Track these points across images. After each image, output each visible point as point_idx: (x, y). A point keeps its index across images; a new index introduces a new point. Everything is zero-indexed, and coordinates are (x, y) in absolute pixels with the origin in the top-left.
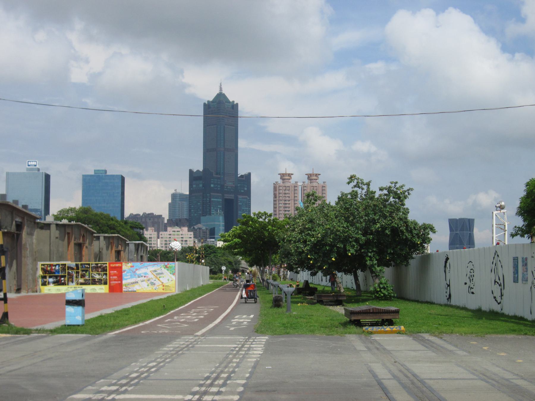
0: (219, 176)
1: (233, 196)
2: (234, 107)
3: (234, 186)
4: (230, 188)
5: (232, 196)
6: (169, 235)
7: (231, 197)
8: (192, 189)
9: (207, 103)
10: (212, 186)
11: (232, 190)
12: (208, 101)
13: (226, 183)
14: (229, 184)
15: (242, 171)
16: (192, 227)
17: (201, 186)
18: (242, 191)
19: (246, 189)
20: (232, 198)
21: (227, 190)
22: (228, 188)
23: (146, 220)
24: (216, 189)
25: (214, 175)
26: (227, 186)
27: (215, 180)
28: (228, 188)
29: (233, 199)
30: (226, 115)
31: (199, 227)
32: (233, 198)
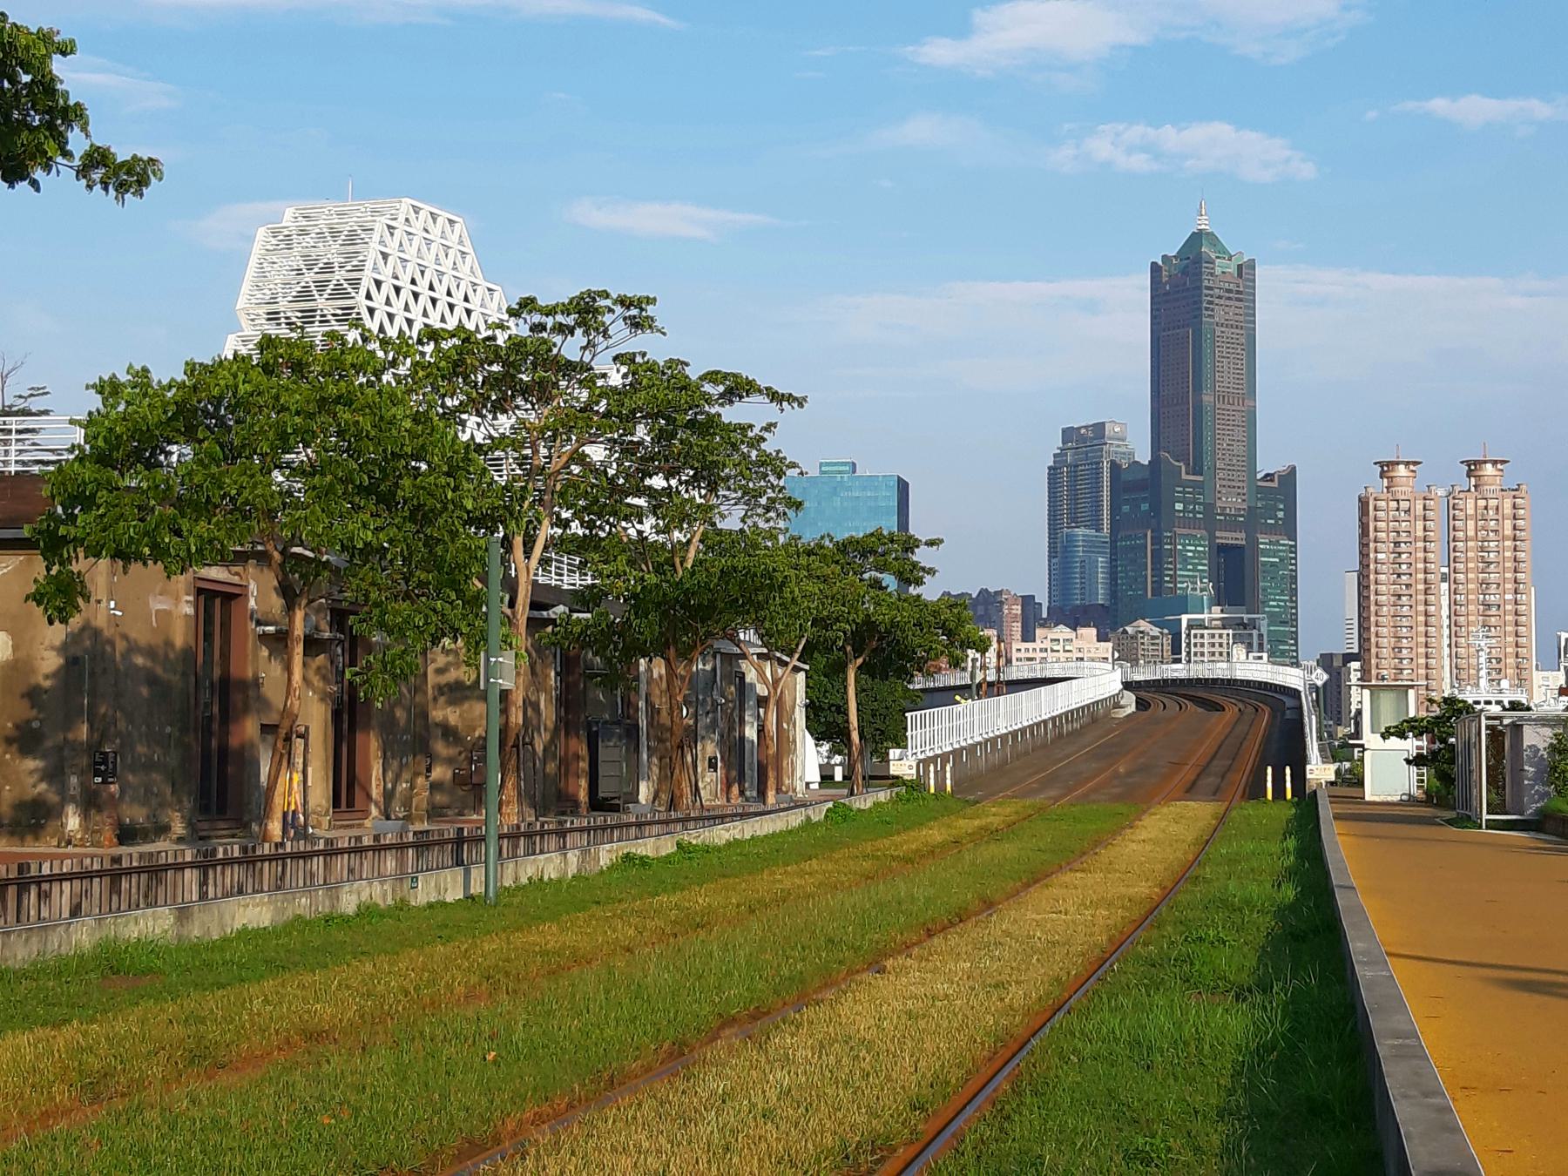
0: (1200, 478)
2: (1246, 271)
4: (1233, 512)
5: (1238, 535)
6: (1041, 650)
7: (1236, 539)
8: (1118, 518)
9: (1160, 263)
10: (1179, 506)
11: (1242, 519)
12: (1164, 257)
13: (1219, 498)
14: (1231, 502)
15: (1267, 463)
16: (1121, 629)
17: (1145, 507)
18: (1269, 521)
19: (1281, 514)
21: (1222, 518)
22: (1228, 511)
23: (986, 610)
24: (1191, 515)
25: (1184, 476)
26: (1225, 508)
27: (1187, 490)
28: (1228, 511)
29: (1241, 548)
30: (1220, 297)
31: (1141, 629)
32: (1244, 543)
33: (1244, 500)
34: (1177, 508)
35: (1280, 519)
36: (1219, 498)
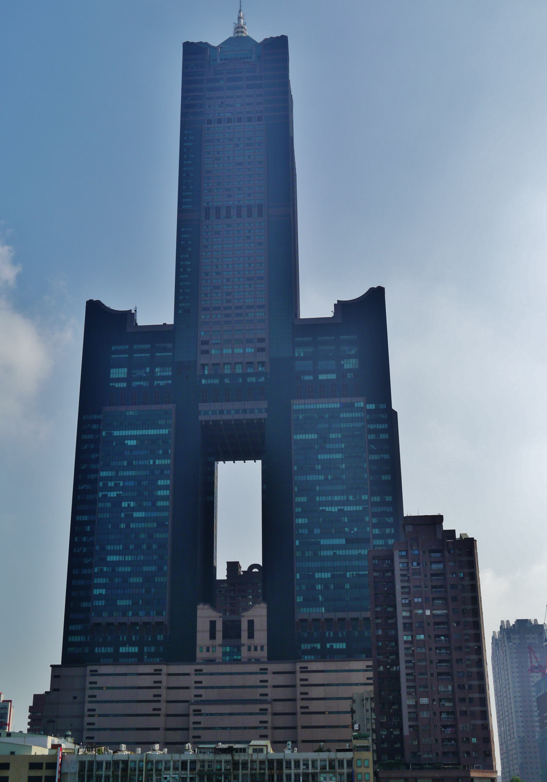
1: (264, 405)
3: (263, 357)
4: (239, 370)
13: (207, 352)
18: (322, 377)
19: (350, 364)
20: (249, 416)
21: (216, 381)
32: (264, 415)
33: (262, 350)
34: (111, 376)
35: (350, 370)
36: (207, 352)
